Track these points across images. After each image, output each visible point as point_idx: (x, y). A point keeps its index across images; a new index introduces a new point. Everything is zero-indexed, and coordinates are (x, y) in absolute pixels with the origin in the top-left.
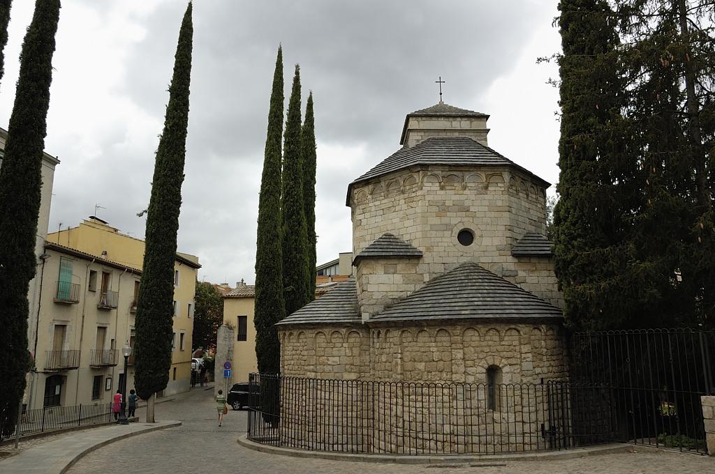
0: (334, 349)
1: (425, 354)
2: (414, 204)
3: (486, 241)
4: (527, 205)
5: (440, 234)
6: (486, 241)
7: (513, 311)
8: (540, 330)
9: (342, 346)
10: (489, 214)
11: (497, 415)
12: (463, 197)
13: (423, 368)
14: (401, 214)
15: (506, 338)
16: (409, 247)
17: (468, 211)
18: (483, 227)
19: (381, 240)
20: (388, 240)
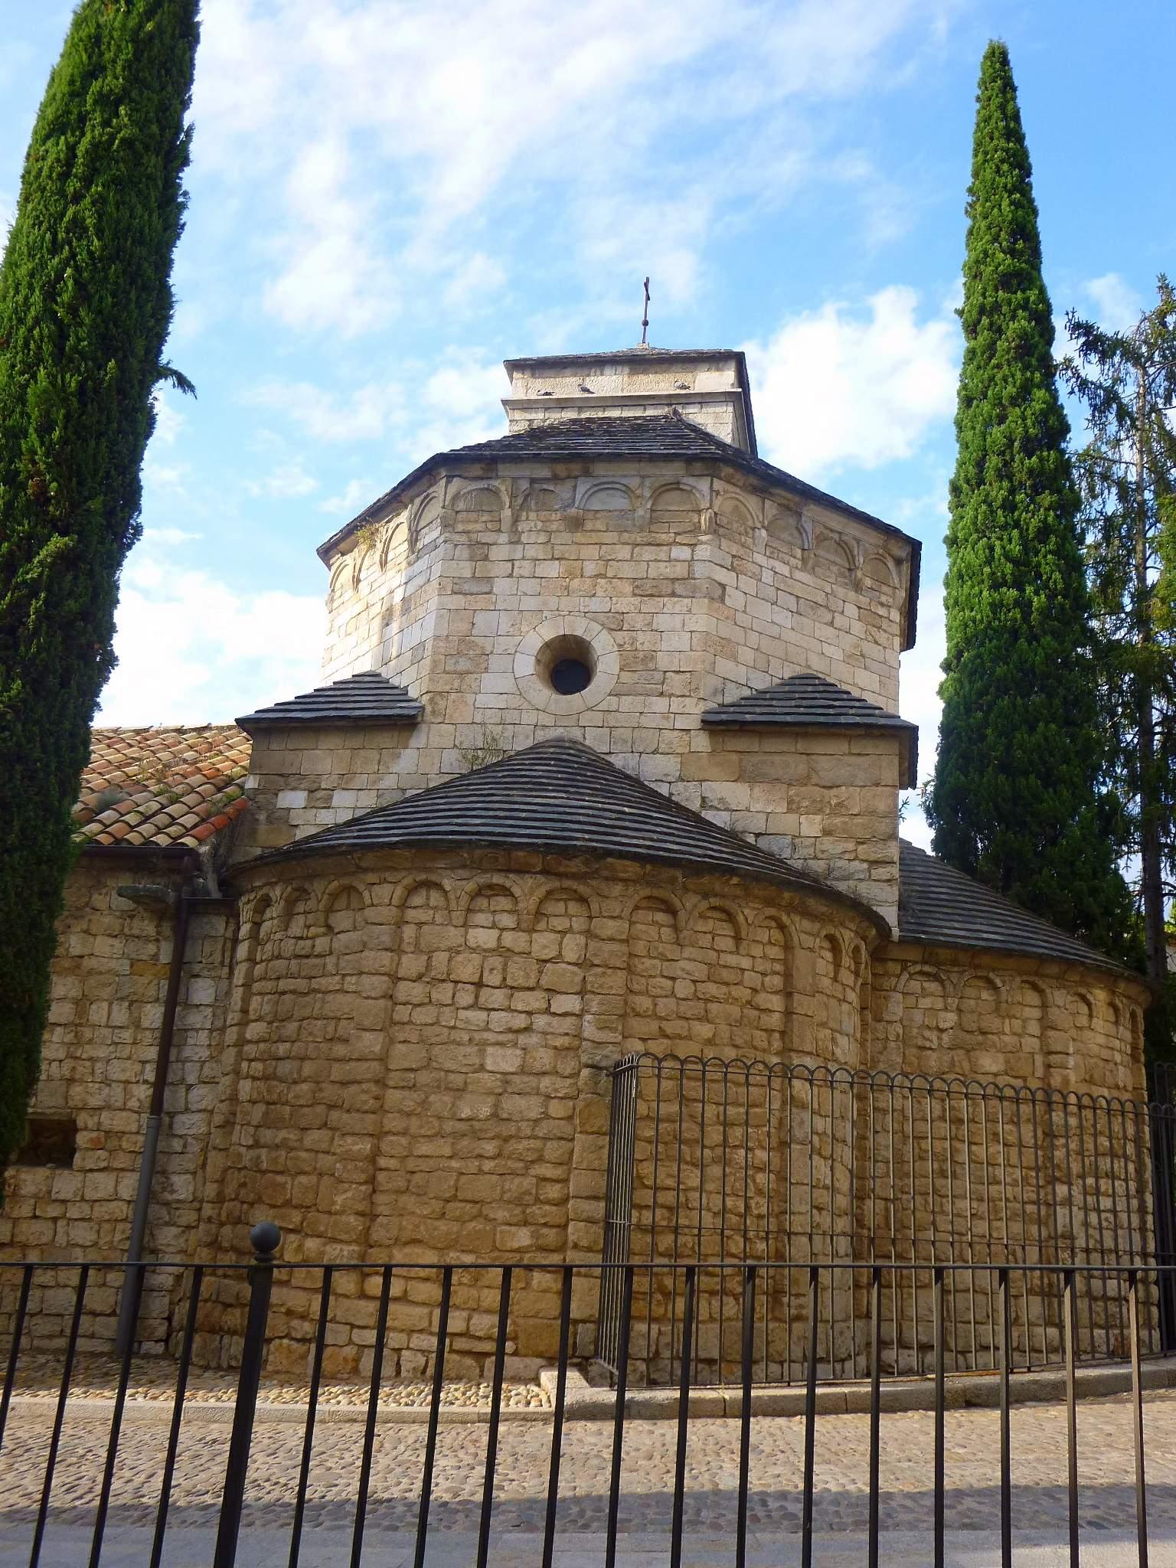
14: (848, 641)
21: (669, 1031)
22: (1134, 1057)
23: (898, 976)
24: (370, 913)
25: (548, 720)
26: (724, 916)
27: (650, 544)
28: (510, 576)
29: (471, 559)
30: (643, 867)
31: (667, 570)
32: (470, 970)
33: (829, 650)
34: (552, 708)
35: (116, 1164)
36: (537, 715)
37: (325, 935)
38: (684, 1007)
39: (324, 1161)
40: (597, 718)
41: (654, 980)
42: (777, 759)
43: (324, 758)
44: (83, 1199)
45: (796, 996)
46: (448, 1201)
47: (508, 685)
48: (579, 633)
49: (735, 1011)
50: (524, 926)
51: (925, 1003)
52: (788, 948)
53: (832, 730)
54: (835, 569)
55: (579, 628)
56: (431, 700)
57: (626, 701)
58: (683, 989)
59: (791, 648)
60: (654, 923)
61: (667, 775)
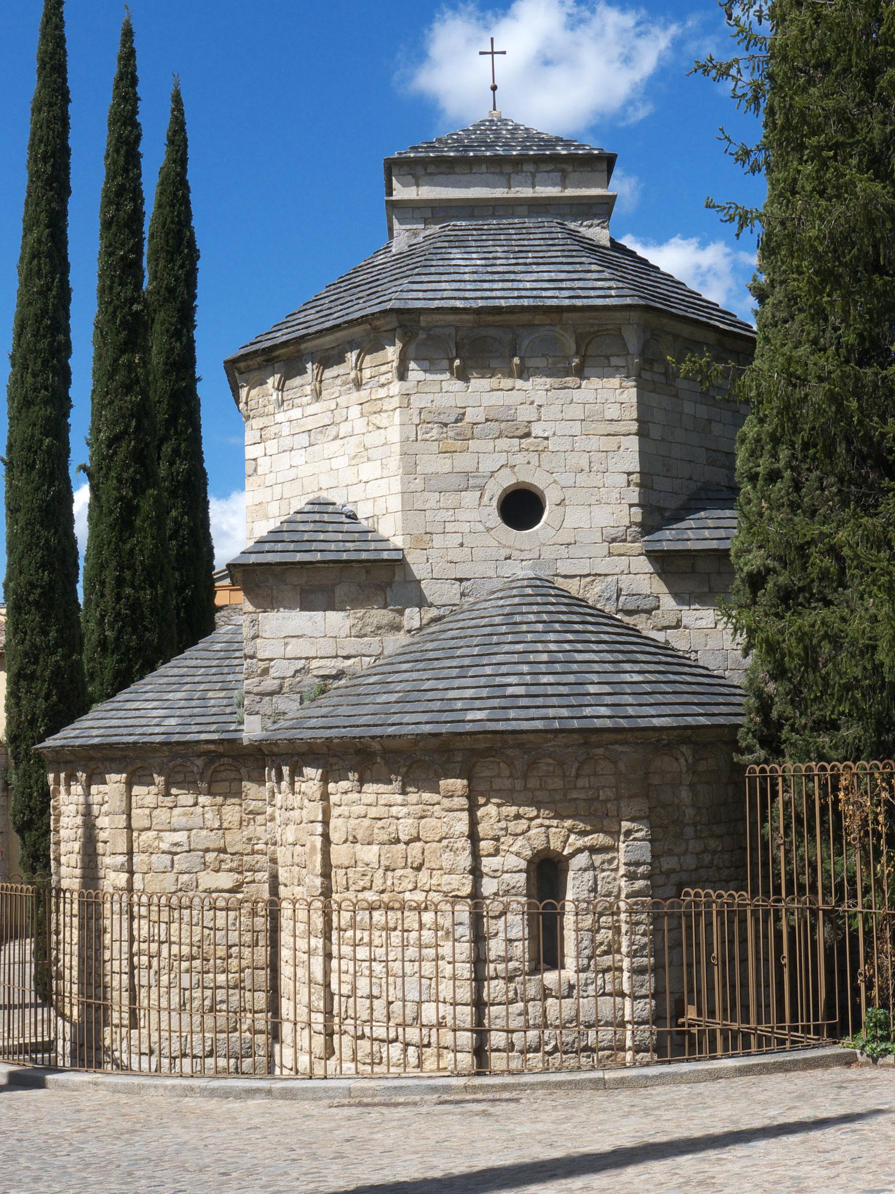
0: (177, 811)
1: (380, 823)
2: (381, 420)
3: (575, 517)
4: (702, 411)
5: (449, 499)
6: (575, 517)
7: (603, 711)
8: (677, 759)
9: (196, 804)
10: (581, 443)
11: (550, 978)
12: (515, 397)
13: (375, 859)
15: (582, 782)
16: (370, 536)
17: (528, 435)
18: (567, 479)
19: (299, 517)
20: (317, 517)
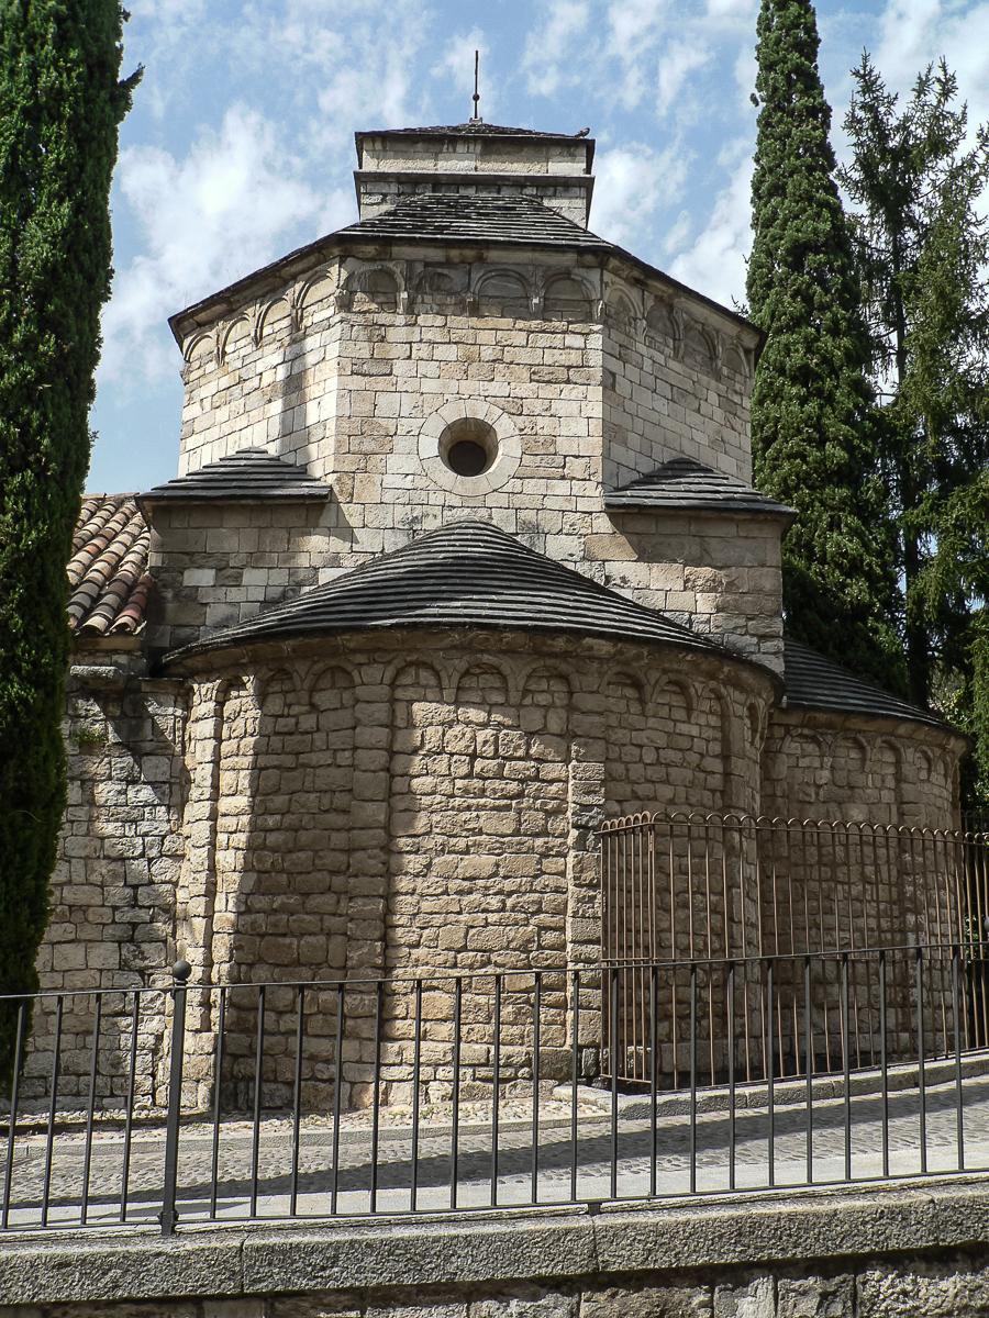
2: (737, 423)
14: (712, 427)
21: (640, 793)
22: (953, 804)
23: (783, 739)
24: (361, 692)
25: (456, 501)
26: (678, 690)
27: (544, 332)
28: (409, 358)
29: (369, 340)
30: (615, 645)
31: (563, 358)
32: (463, 743)
33: (699, 436)
34: (459, 489)
35: (83, 936)
36: (450, 499)
37: (309, 713)
38: (650, 772)
39: (333, 923)
40: (503, 500)
41: (626, 748)
42: (673, 541)
43: (231, 538)
44: (53, 970)
45: (734, 759)
46: (459, 951)
47: (411, 465)
48: (480, 417)
49: (688, 774)
50: (512, 701)
51: (803, 762)
52: (724, 716)
53: (725, 515)
54: (699, 358)
55: (480, 411)
56: (338, 480)
57: (531, 486)
58: (649, 757)
59: (668, 434)
60: (623, 697)
61: (572, 555)
